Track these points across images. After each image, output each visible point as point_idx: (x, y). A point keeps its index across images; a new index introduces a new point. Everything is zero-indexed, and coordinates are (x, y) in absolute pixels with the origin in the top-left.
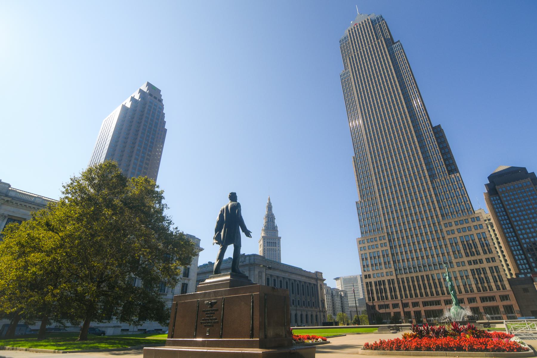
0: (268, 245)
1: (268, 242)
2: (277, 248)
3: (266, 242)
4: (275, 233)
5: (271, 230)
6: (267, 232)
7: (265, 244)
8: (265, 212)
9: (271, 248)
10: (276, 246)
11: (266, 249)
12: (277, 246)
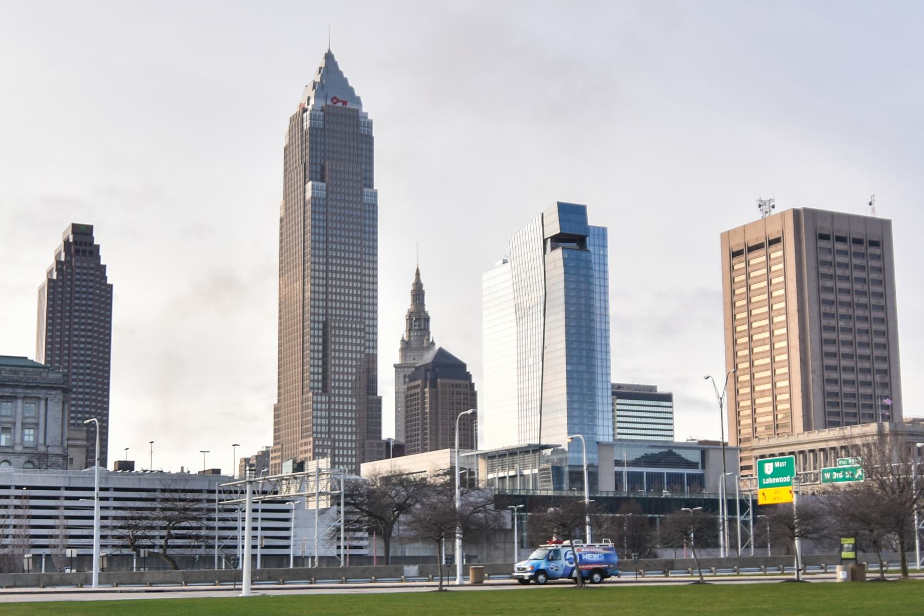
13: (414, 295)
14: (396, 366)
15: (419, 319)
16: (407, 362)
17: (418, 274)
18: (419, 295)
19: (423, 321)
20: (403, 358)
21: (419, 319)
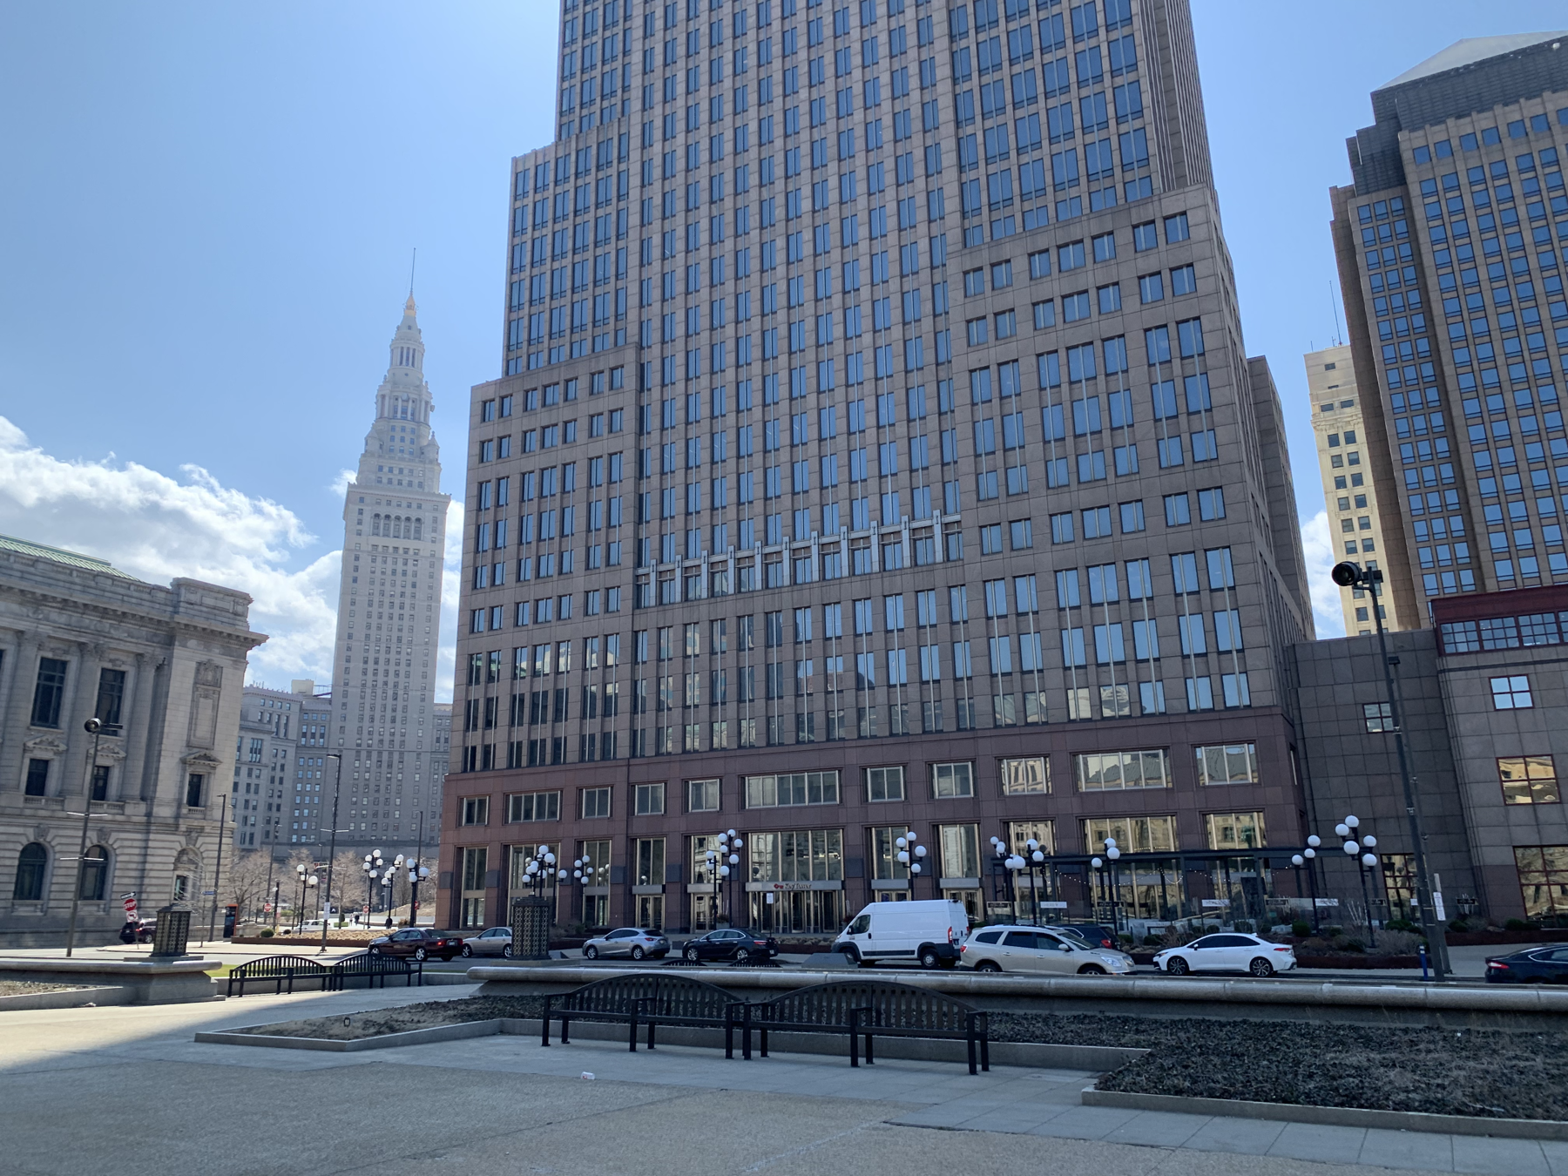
0: (376, 527)
1: (377, 516)
2: (425, 547)
3: (367, 518)
5: (402, 459)
6: (381, 468)
7: (360, 523)
8: (380, 365)
9: (391, 542)
12: (427, 533)
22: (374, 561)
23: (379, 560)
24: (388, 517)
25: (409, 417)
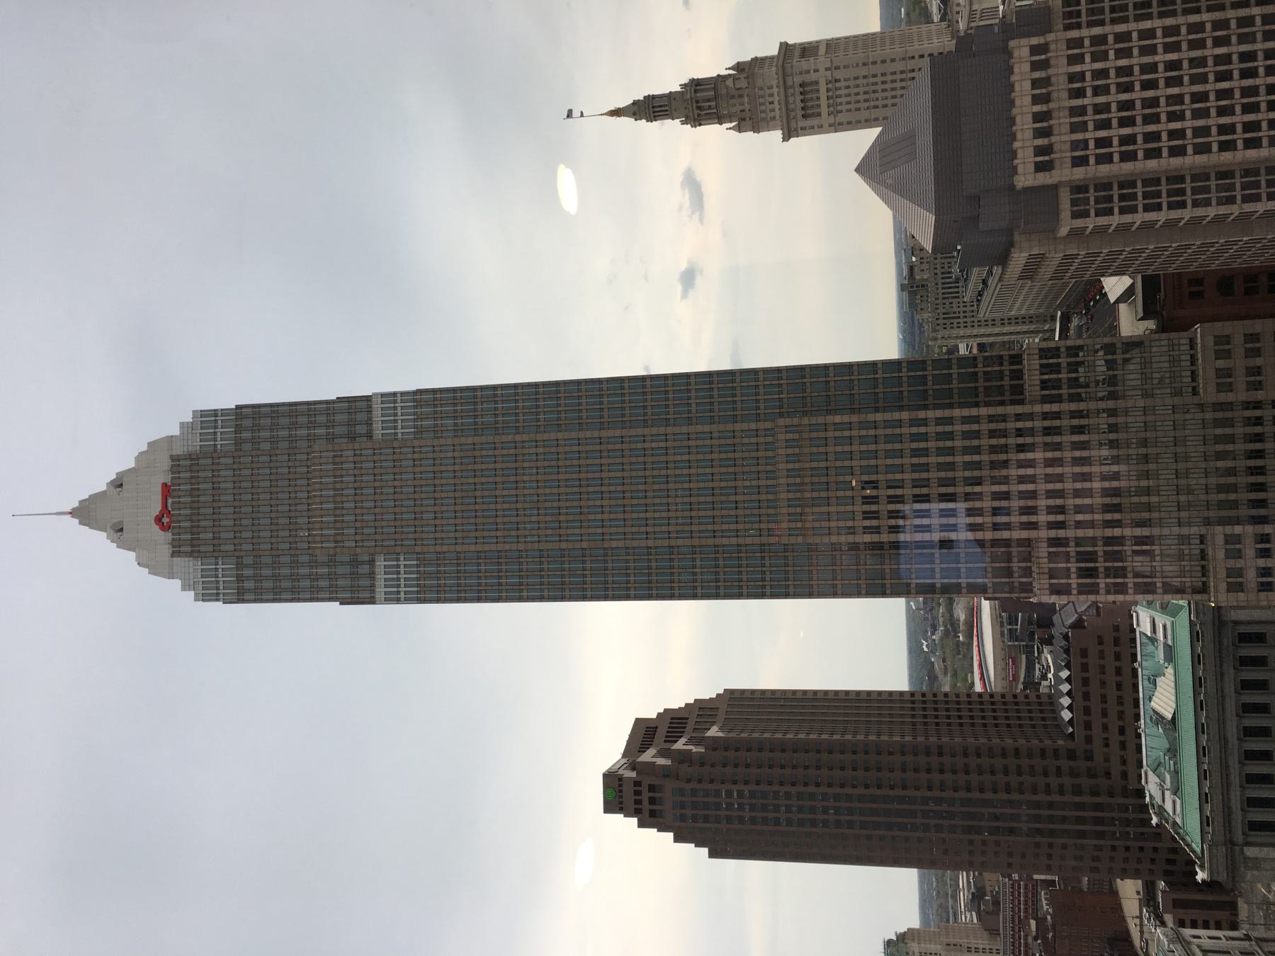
0: (812, 115)
3: (809, 123)
4: (761, 89)
6: (763, 119)
7: (812, 127)
9: (824, 102)
10: (817, 83)
11: (832, 120)
13: (655, 116)
14: (786, 138)
15: (697, 102)
16: (778, 117)
17: (616, 113)
18: (653, 107)
19: (698, 95)
20: (771, 123)
21: (697, 102)
22: (841, 112)
23: (839, 108)
24: (803, 109)
25: (713, 104)
